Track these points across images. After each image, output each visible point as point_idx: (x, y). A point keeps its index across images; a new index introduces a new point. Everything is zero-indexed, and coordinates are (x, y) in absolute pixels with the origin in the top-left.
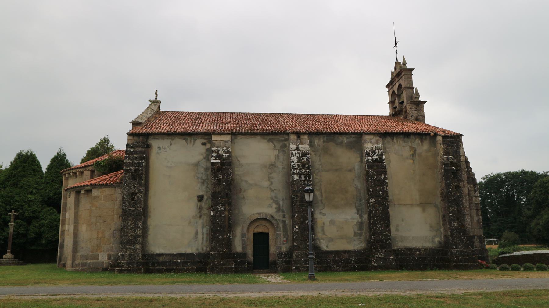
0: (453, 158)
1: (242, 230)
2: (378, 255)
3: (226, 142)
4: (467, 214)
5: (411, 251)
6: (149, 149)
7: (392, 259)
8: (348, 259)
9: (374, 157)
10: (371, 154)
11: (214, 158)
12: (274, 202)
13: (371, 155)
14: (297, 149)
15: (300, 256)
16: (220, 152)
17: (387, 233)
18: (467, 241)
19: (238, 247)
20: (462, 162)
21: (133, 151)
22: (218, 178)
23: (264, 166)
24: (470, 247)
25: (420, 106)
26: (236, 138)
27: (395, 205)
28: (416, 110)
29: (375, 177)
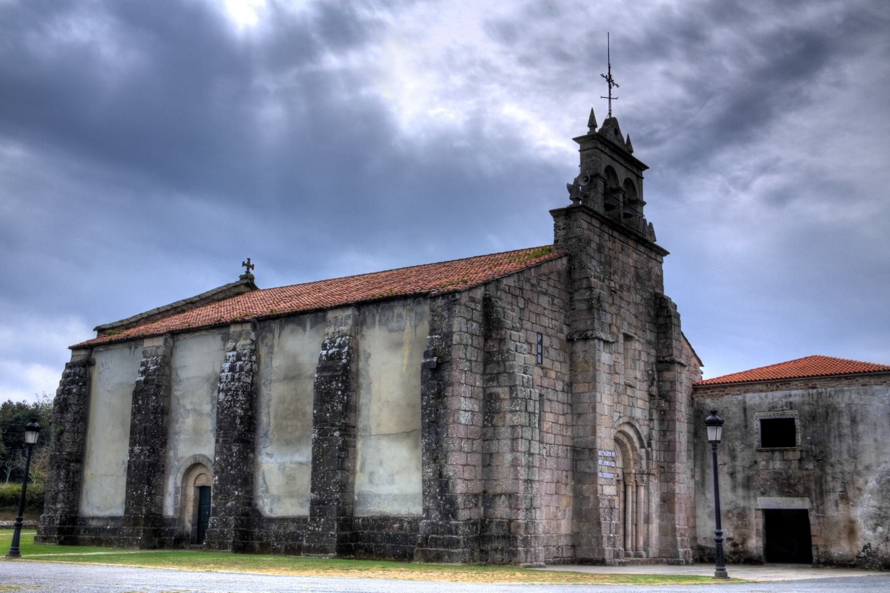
0: (441, 339)
1: (175, 483)
2: (314, 527)
3: (158, 347)
4: (452, 451)
5: (384, 521)
6: (92, 368)
7: (332, 535)
8: (295, 533)
9: (330, 352)
10: (328, 345)
11: (140, 375)
12: (261, 437)
13: (328, 348)
14: (234, 349)
15: (215, 525)
16: (148, 365)
17: (331, 487)
18: (445, 505)
19: (169, 510)
20: (455, 345)
21: (69, 373)
22: (138, 404)
23: (207, 379)
24: (450, 515)
25: (573, 217)
26: (178, 340)
27: (371, 435)
28: (565, 226)
29: (323, 387)
